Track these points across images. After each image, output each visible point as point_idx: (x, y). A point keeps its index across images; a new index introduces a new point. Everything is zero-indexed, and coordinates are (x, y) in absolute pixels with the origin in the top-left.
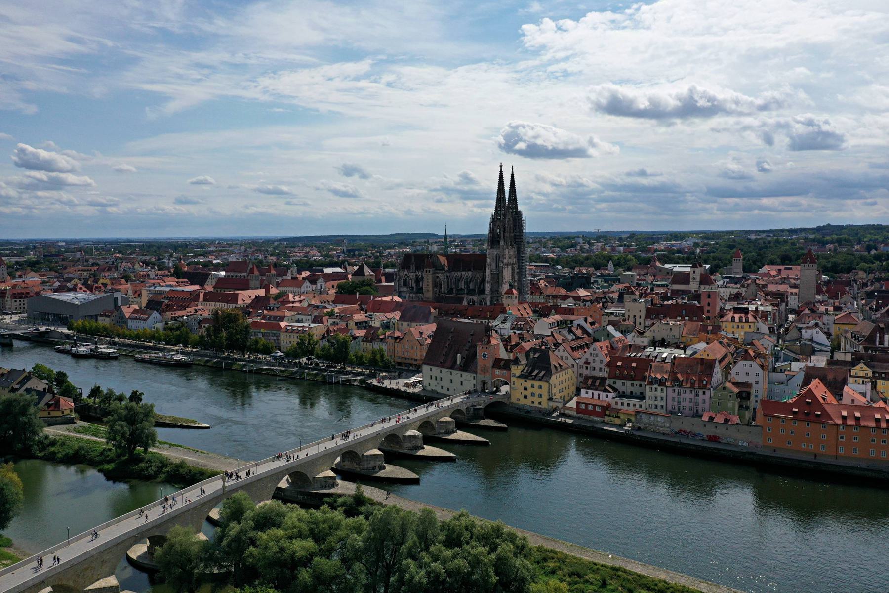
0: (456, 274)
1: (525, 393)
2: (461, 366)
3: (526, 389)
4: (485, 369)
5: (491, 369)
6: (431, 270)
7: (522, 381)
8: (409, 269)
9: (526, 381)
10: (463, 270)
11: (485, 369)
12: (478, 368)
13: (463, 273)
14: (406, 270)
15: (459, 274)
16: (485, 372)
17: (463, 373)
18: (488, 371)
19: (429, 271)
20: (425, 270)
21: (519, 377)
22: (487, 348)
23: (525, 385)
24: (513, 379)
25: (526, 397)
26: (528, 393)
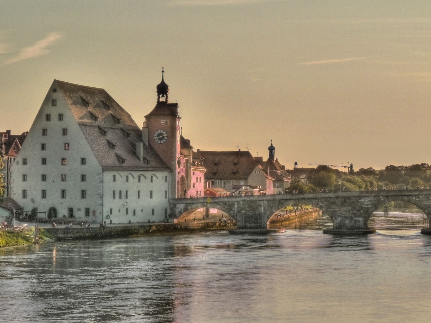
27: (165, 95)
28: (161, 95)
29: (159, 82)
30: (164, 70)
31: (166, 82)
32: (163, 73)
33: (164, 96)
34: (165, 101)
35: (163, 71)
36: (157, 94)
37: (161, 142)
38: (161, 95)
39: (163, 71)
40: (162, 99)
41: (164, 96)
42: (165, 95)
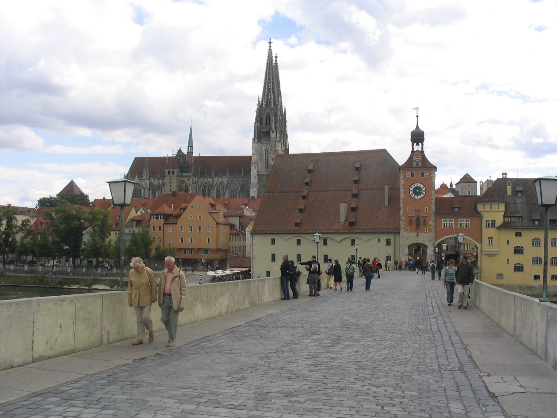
0: (206, 180)
1: (518, 259)
2: (352, 224)
3: (518, 251)
4: (418, 219)
5: (433, 218)
6: (175, 170)
7: (510, 235)
8: (141, 176)
9: (519, 234)
10: (217, 174)
11: (418, 219)
12: (403, 218)
13: (216, 179)
14: (137, 177)
15: (210, 180)
16: (418, 225)
17: (354, 236)
18: (425, 223)
19: (173, 172)
20: (166, 171)
21: (504, 226)
22: (423, 174)
23: (517, 242)
24: (487, 232)
25: (519, 268)
26: (524, 260)
27: (420, 144)
28: (415, 144)
29: (414, 128)
30: (418, 115)
31: (421, 128)
32: (417, 118)
33: (419, 145)
34: (420, 150)
35: (417, 116)
36: (411, 143)
37: (418, 197)
38: (415, 144)
39: (417, 116)
40: (418, 148)
41: (419, 145)
42: (420, 144)
